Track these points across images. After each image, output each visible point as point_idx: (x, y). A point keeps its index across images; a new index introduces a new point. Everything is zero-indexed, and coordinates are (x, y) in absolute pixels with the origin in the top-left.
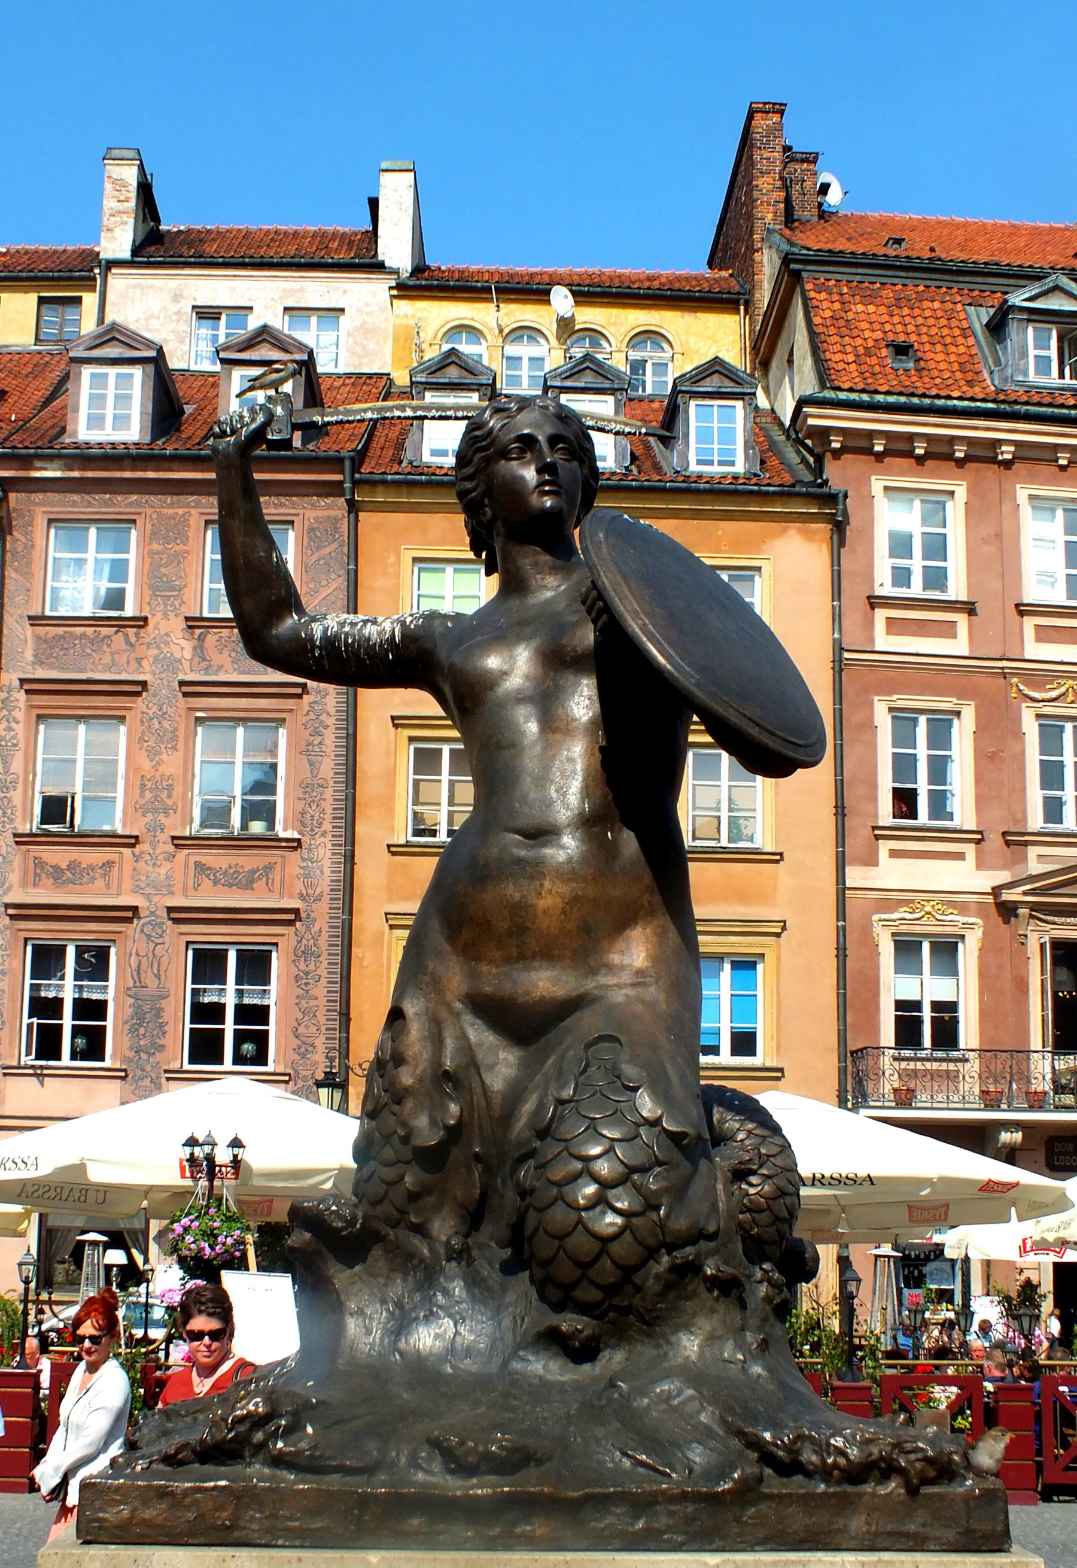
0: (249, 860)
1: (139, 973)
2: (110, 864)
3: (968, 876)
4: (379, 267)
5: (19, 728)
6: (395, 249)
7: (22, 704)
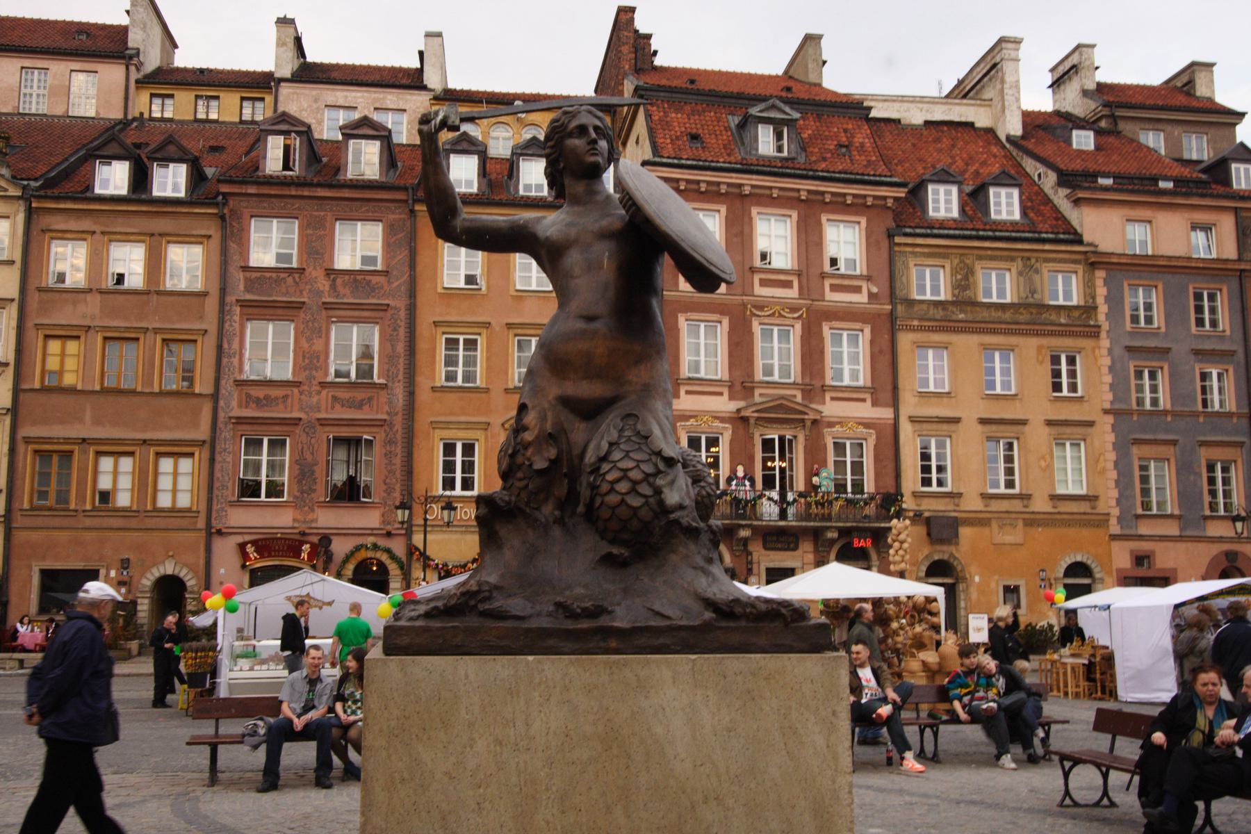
0: (360, 395)
2: (286, 397)
3: (724, 404)
4: (425, 88)
5: (237, 325)
6: (432, 79)
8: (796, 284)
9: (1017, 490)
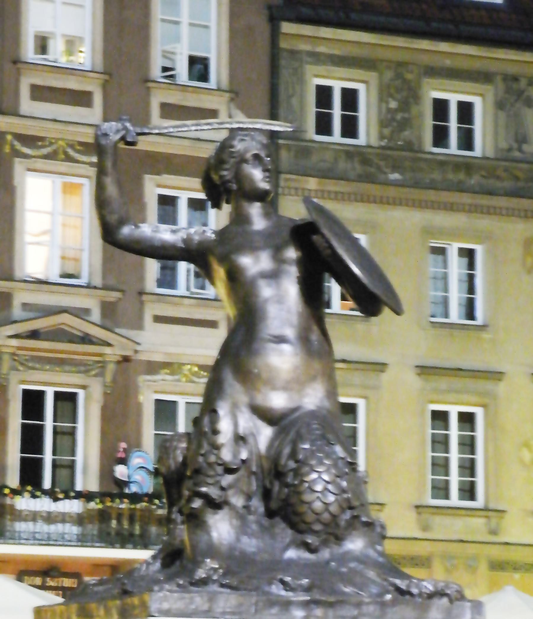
8: (98, 99)
9: (479, 503)
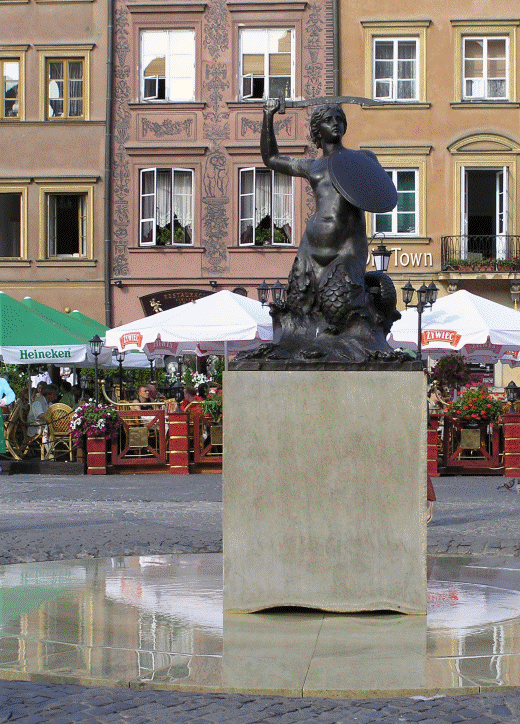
1: (210, 189)
7: (130, 21)
